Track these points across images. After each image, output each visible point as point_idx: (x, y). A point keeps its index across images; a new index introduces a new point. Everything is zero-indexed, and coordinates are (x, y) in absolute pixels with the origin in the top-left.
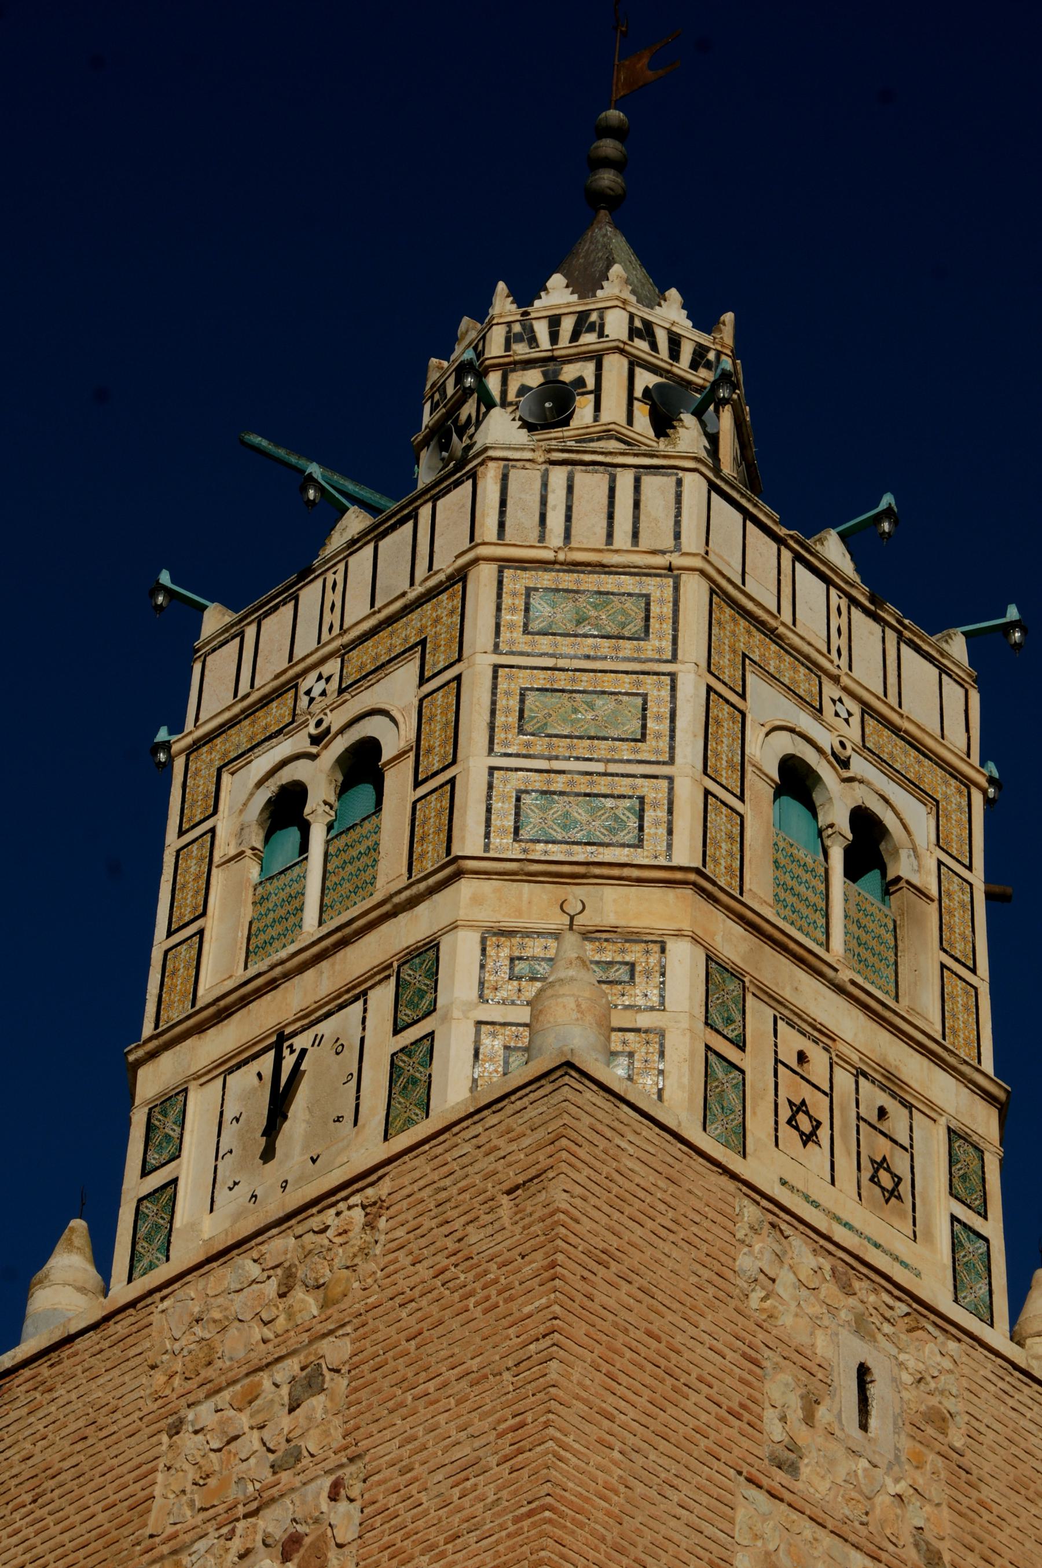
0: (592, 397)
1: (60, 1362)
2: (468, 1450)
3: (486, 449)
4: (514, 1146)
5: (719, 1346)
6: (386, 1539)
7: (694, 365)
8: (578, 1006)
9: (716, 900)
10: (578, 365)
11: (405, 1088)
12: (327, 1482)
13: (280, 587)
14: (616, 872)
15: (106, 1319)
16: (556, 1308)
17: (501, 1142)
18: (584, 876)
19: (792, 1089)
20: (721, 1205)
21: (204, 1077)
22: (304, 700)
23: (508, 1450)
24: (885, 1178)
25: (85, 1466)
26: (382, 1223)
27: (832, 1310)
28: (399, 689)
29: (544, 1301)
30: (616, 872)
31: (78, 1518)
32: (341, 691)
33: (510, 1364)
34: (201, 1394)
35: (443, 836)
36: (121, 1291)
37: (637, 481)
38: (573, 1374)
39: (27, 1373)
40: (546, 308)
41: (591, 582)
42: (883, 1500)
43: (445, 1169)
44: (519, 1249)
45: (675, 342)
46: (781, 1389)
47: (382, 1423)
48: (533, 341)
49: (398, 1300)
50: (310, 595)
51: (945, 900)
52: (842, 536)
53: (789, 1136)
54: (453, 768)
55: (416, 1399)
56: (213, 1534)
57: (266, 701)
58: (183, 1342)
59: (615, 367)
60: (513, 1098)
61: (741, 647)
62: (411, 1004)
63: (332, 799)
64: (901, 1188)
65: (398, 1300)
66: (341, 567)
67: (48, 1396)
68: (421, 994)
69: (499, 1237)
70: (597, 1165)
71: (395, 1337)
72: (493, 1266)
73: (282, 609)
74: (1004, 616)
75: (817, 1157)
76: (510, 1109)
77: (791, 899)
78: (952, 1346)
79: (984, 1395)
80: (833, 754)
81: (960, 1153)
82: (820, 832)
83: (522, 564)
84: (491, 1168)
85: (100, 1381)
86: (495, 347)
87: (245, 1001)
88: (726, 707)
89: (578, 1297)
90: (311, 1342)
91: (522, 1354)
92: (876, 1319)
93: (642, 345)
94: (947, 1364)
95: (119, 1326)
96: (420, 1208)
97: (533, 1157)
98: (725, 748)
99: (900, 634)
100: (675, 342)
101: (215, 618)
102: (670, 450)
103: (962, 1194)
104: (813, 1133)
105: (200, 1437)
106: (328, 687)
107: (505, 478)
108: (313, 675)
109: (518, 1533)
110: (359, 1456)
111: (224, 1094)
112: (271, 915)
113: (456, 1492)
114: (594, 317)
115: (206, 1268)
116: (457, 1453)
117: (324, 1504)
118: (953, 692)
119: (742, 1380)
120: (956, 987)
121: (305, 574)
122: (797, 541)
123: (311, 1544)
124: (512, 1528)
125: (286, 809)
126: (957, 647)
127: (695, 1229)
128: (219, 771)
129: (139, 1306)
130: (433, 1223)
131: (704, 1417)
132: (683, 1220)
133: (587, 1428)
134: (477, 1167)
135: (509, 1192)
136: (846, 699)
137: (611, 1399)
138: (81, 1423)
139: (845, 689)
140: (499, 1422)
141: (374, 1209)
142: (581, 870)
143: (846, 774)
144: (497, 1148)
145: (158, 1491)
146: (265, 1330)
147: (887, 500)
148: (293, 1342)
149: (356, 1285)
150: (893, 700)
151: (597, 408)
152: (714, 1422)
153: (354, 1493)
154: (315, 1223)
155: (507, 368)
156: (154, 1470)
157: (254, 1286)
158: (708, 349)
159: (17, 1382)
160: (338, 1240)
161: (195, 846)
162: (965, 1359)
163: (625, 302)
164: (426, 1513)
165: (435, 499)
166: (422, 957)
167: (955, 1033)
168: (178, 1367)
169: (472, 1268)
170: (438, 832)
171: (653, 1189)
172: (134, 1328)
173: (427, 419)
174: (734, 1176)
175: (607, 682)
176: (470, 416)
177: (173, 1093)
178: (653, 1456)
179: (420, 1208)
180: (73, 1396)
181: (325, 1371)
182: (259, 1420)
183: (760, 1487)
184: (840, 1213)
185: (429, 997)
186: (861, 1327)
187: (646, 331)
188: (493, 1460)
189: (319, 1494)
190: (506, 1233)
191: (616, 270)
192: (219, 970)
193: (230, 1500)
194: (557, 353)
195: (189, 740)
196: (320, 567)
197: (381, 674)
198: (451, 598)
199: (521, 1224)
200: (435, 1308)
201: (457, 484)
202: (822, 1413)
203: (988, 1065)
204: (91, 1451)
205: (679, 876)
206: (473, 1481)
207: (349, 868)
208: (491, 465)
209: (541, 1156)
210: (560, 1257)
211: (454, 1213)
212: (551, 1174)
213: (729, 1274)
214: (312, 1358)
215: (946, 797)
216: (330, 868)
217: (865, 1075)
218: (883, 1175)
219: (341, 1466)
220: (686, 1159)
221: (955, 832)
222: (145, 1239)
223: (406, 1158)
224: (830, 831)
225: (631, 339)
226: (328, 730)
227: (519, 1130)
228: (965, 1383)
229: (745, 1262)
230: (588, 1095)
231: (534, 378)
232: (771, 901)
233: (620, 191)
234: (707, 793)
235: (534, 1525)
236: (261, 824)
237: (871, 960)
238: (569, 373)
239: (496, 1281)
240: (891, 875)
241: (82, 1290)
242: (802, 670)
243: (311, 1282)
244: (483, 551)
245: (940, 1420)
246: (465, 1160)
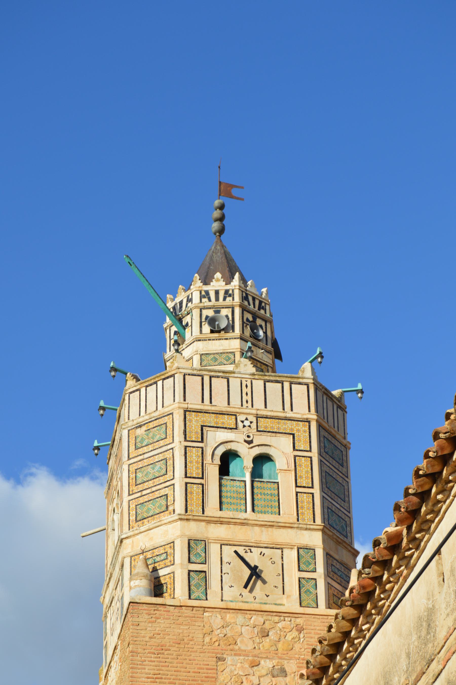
11: (306, 592)
22: (240, 425)
35: (311, 511)
39: (145, 606)
41: (333, 441)
48: (249, 305)
62: (304, 563)
66: (249, 381)
68: (310, 564)
87: (229, 523)
106: (252, 425)
111: (221, 551)
114: (263, 304)
159: (140, 608)
166: (309, 550)
177: (200, 539)
197: (274, 434)
201: (300, 384)
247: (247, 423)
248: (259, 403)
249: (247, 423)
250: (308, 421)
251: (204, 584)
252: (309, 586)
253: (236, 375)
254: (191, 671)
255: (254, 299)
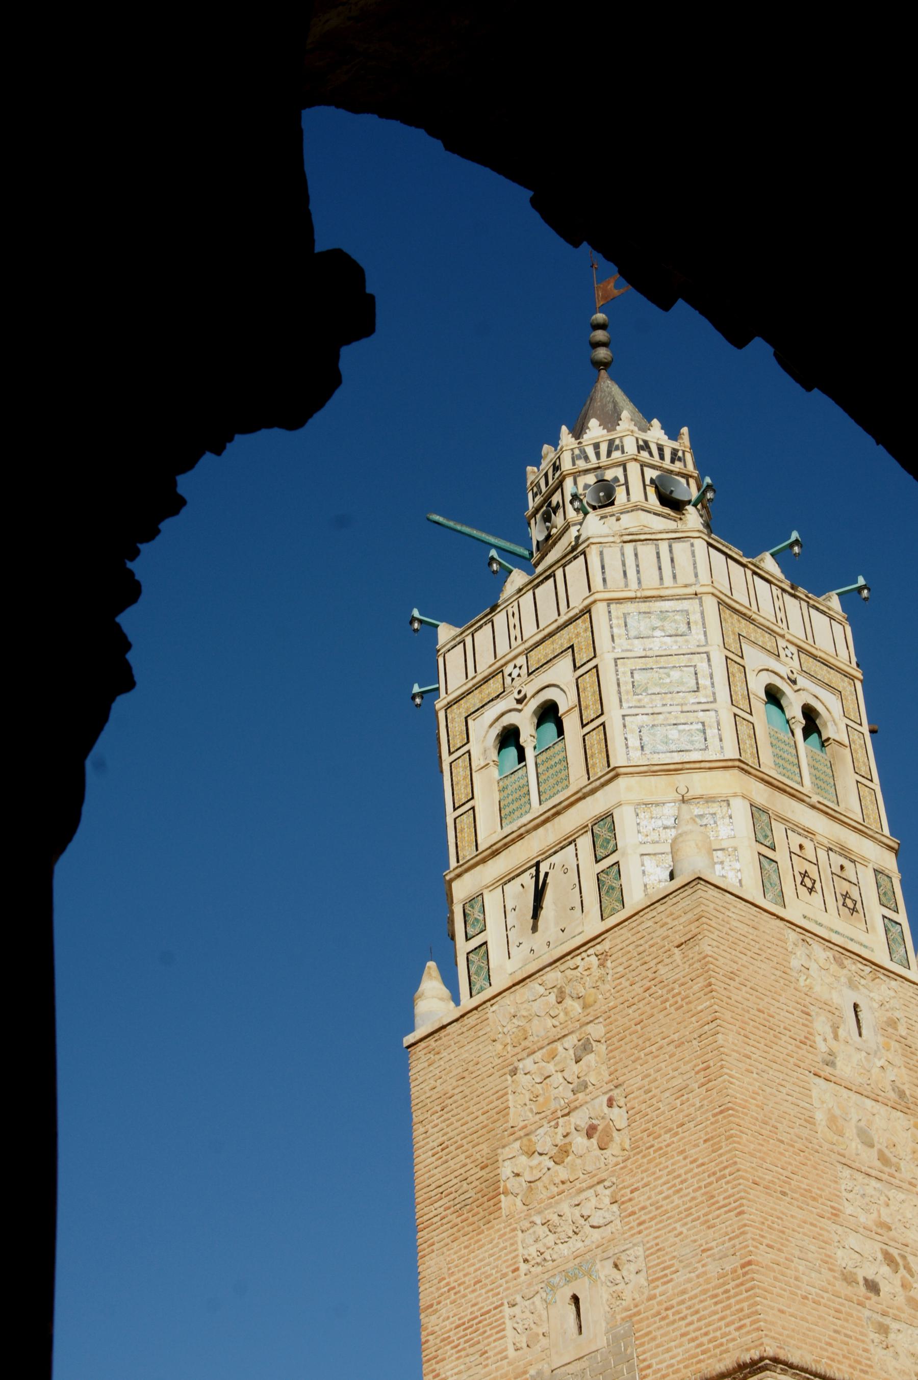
0: (624, 487)
1: (440, 1039)
2: (680, 1081)
3: (588, 538)
4: (676, 922)
5: (790, 1009)
6: (643, 1126)
7: (673, 461)
8: (697, 845)
9: (750, 773)
10: (614, 469)
11: (608, 892)
12: (605, 1099)
13: (481, 615)
14: (697, 765)
15: (462, 1016)
16: (716, 1007)
17: (669, 920)
18: (681, 770)
19: (801, 866)
20: (779, 936)
21: (491, 886)
22: (508, 680)
23: (703, 1080)
24: (849, 903)
25: (467, 1092)
26: (609, 964)
27: (837, 978)
28: (562, 672)
29: (708, 1003)
30: (697, 765)
31: (469, 1118)
32: (529, 674)
33: (696, 1036)
34: (525, 1054)
35: (604, 755)
36: (467, 1003)
37: (670, 546)
38: (728, 1039)
39: (422, 1044)
40: (590, 439)
42: (875, 1071)
43: (639, 935)
44: (689, 977)
45: (661, 449)
46: (821, 1025)
47: (629, 1068)
48: (586, 458)
49: (626, 1004)
50: (500, 619)
51: (853, 746)
52: (772, 555)
53: (802, 890)
54: (602, 717)
55: (646, 1055)
56: (546, 1125)
57: (486, 680)
58: (509, 1027)
59: (633, 469)
60: (671, 896)
61: (737, 630)
62: (602, 846)
63: (533, 733)
64: (857, 906)
65: (626, 1004)
66: (515, 604)
67: (438, 1057)
68: (608, 842)
69: (677, 970)
70: (720, 928)
71: (629, 1024)
72: (676, 985)
73: (485, 627)
74: (857, 582)
75: (817, 898)
76: (670, 902)
77: (782, 762)
78: (893, 983)
79: (911, 1006)
80: (789, 678)
81: (880, 881)
82: (788, 722)
83: (619, 601)
84: (665, 934)
85: (466, 1048)
86: (566, 465)
87: (506, 846)
88: (736, 665)
89: (725, 999)
90: (581, 1027)
91: (701, 1031)
92: (857, 978)
93: (644, 454)
94: (892, 993)
95: (470, 1020)
96: (629, 956)
97: (687, 929)
98: (739, 688)
99: (808, 603)
100: (661, 449)
101: (445, 633)
102: (685, 529)
103: (886, 903)
104: (813, 887)
105: (528, 1076)
107: (601, 553)
108: (511, 665)
109: (717, 1122)
110: (620, 1085)
112: (511, 797)
113: (678, 1102)
114: (617, 442)
115: (513, 989)
116: (674, 1082)
117: (606, 1110)
118: (837, 628)
119: (803, 1025)
120: (865, 792)
121: (494, 608)
122: (753, 564)
123: (603, 1130)
124: (713, 1120)
125: (509, 737)
126: (834, 603)
127: (769, 951)
128: (466, 718)
129: (479, 1009)
130: (638, 963)
131: (790, 1047)
132: (763, 948)
133: (740, 1065)
134: (657, 933)
135: (678, 946)
136: (790, 646)
137: (748, 1048)
138: (460, 1070)
139: (788, 641)
140: (695, 1066)
141: (603, 956)
142: (679, 766)
143: (796, 687)
144: (666, 924)
145: (511, 1104)
146: (553, 1020)
147: (795, 535)
148: (571, 1027)
149: (600, 996)
150: (810, 641)
151: (628, 493)
152: (795, 1049)
153: (621, 1103)
154: (571, 964)
155: (576, 475)
156: (506, 1094)
157: (543, 998)
158: (677, 451)
159: (418, 1049)
160: (586, 973)
161: (460, 760)
162: (900, 989)
163: (632, 432)
164: (663, 1113)
165: (564, 566)
167: (869, 817)
168: (509, 1041)
169: (664, 987)
170: (600, 752)
171: (747, 935)
172: (479, 1021)
173: (532, 504)
174: (782, 919)
175: (674, 661)
176: (558, 502)
178: (771, 1072)
179: (629, 956)
180: (452, 1056)
181: (592, 1042)
182: (559, 1067)
183: (820, 1077)
184: (832, 927)
185: (612, 843)
186: (852, 985)
187: (644, 446)
188: (696, 1085)
189: (602, 1105)
190: (681, 968)
191: (625, 414)
192: (489, 831)
193: (553, 1109)
194: (601, 465)
195: (445, 702)
196: (503, 603)
198: (584, 622)
199: (688, 963)
200: (648, 1008)
201: (575, 558)
202: (841, 1032)
203: (886, 831)
204: (469, 1084)
205: (730, 764)
206: (686, 1096)
207: (551, 771)
208: (593, 546)
209: (693, 927)
210: (713, 980)
211: (649, 958)
212: (700, 937)
213: (788, 971)
214: (583, 1035)
215: (844, 688)
216: (539, 771)
217: (831, 849)
218: (848, 901)
219: (611, 1090)
220: (759, 915)
221: (851, 705)
222: (475, 974)
223: (616, 929)
224: (793, 720)
225: (639, 452)
226: (525, 697)
227: (677, 914)
228: (901, 1001)
229: (795, 963)
230: (710, 892)
231: (591, 479)
232: (773, 766)
233: (610, 359)
234: (735, 715)
235: (725, 1118)
236: (495, 747)
237: (824, 786)
238: (609, 475)
239: (679, 993)
240: (824, 738)
241: (441, 999)
242: (767, 635)
243: (575, 996)
244: (597, 596)
245: (893, 1023)
246: (650, 930)
247: (515, 673)
248: (529, 629)
249: (515, 673)
250: (587, 611)
251: (484, 965)
252: (608, 880)
253: (499, 609)
254: (480, 1112)
255: (596, 446)
